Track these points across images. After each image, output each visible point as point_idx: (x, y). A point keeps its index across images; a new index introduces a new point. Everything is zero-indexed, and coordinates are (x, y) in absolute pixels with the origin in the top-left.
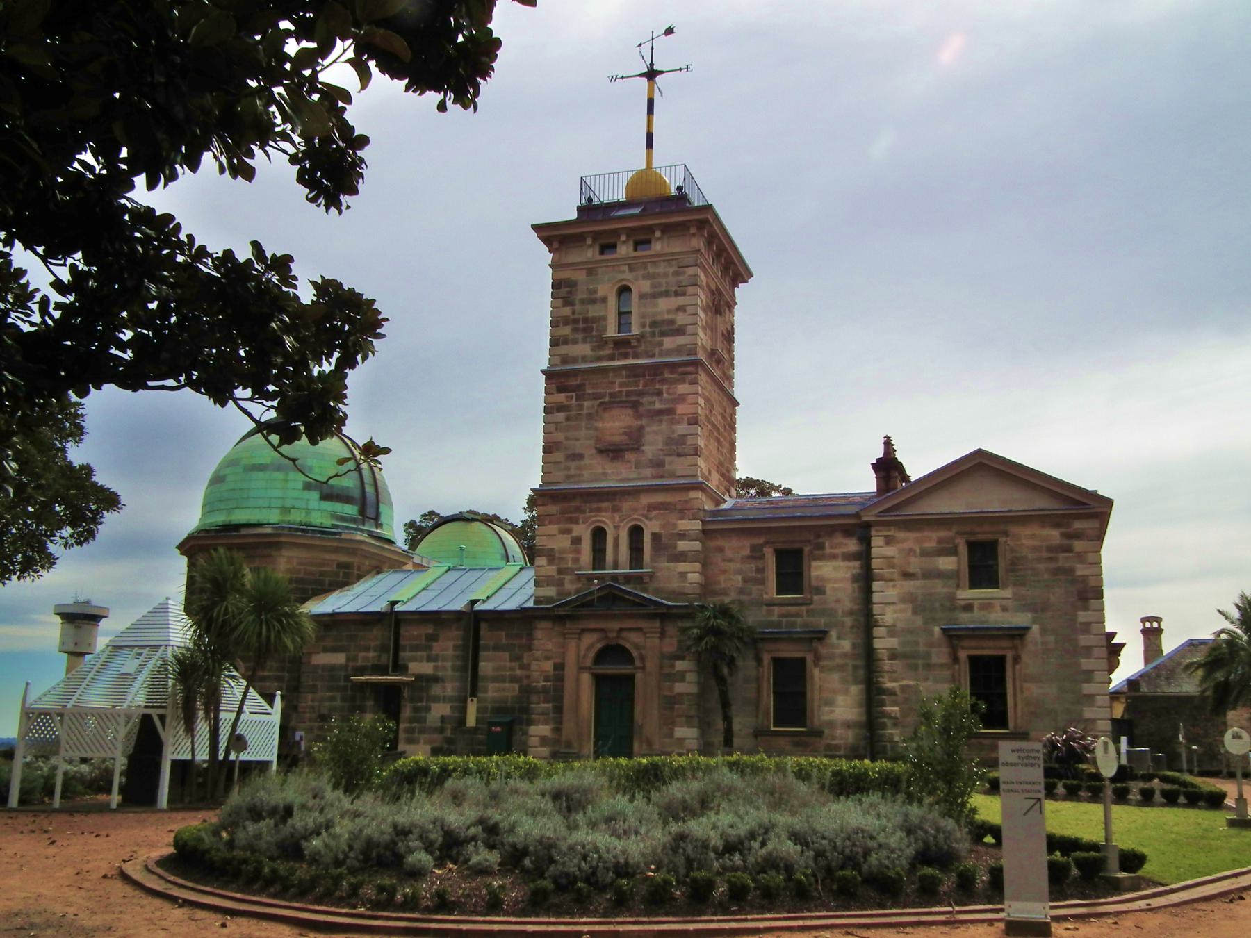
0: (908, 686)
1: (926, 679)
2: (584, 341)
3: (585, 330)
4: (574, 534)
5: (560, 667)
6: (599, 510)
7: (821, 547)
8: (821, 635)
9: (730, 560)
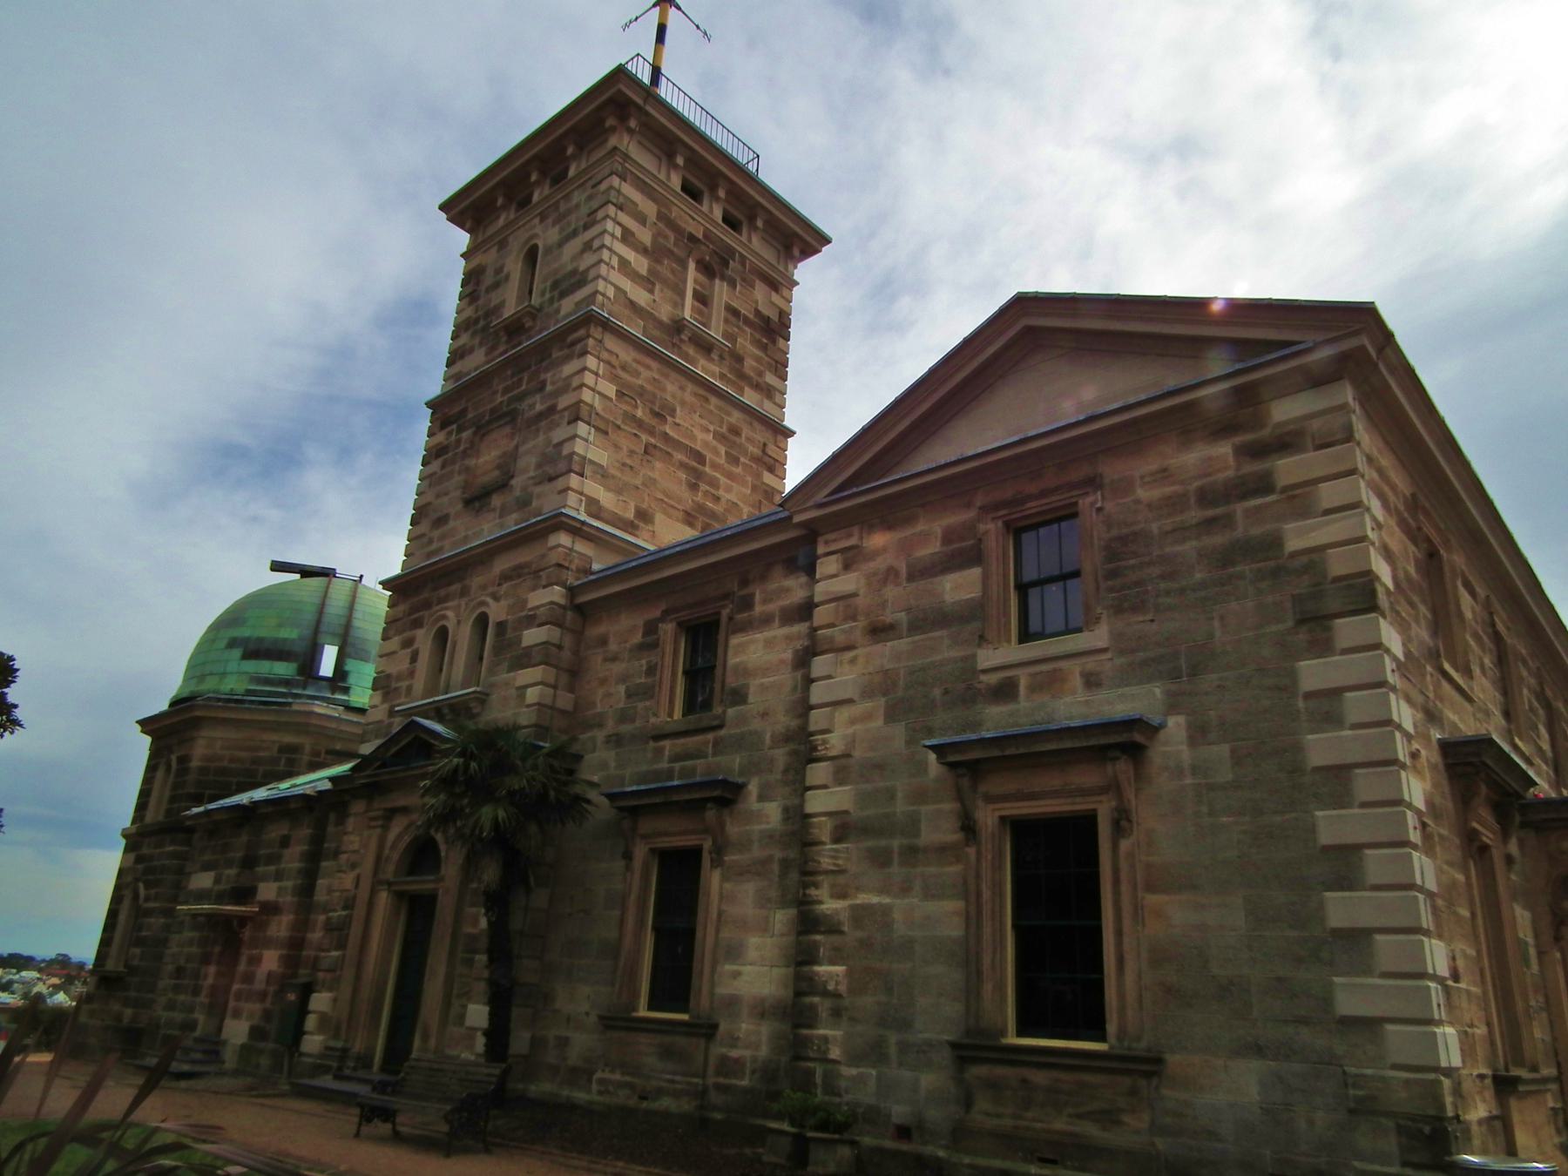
0: (867, 908)
1: (905, 890)
7: (747, 604)
8: (727, 794)
9: (614, 659)
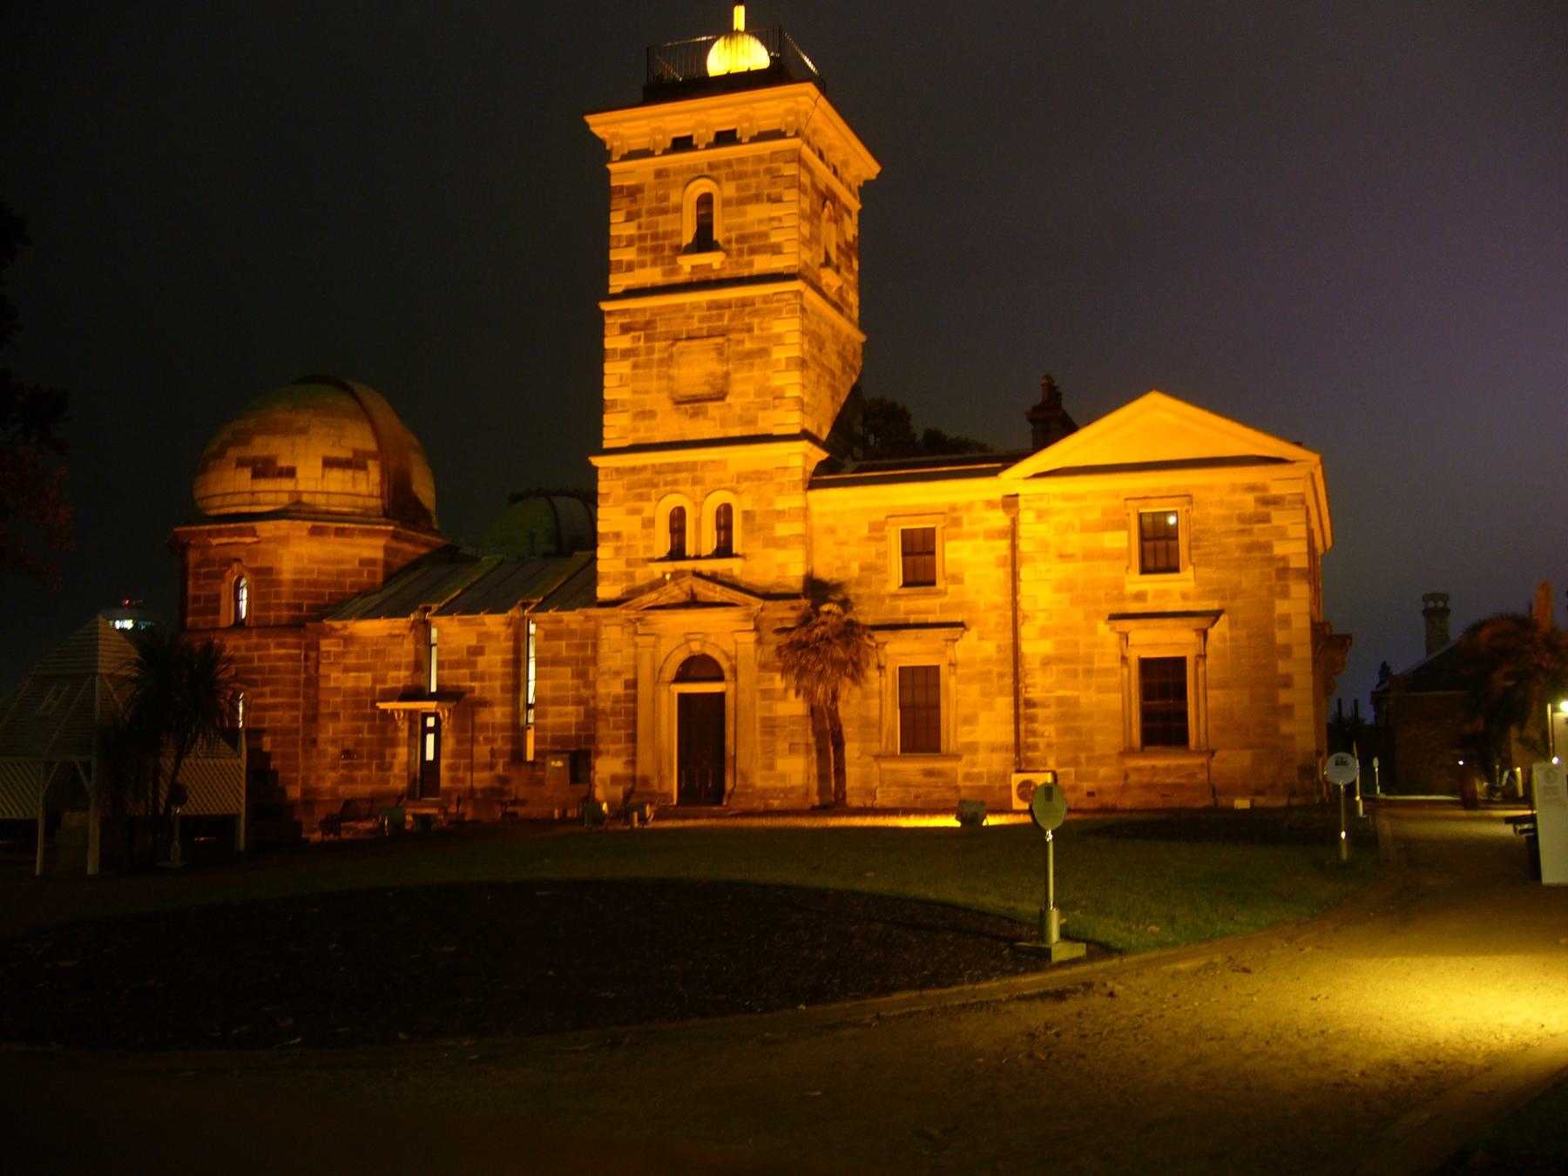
1: (1088, 687)
2: (654, 263)
3: (654, 249)
4: (646, 514)
5: (632, 684)
6: (675, 482)
7: (957, 522)
